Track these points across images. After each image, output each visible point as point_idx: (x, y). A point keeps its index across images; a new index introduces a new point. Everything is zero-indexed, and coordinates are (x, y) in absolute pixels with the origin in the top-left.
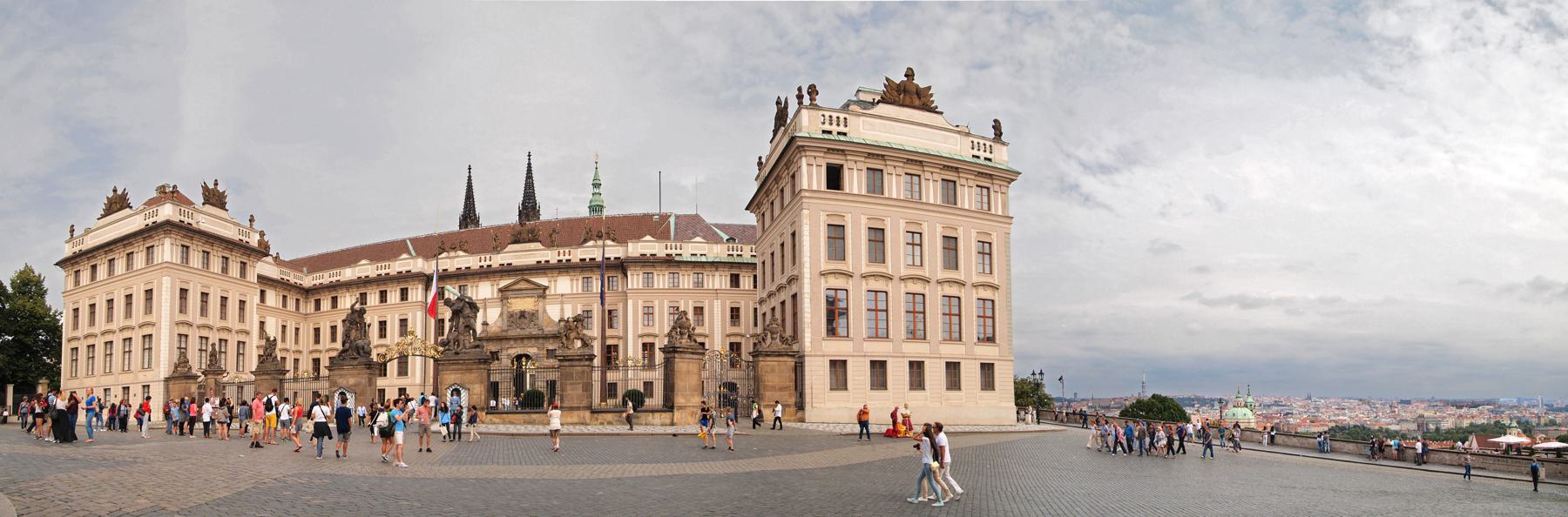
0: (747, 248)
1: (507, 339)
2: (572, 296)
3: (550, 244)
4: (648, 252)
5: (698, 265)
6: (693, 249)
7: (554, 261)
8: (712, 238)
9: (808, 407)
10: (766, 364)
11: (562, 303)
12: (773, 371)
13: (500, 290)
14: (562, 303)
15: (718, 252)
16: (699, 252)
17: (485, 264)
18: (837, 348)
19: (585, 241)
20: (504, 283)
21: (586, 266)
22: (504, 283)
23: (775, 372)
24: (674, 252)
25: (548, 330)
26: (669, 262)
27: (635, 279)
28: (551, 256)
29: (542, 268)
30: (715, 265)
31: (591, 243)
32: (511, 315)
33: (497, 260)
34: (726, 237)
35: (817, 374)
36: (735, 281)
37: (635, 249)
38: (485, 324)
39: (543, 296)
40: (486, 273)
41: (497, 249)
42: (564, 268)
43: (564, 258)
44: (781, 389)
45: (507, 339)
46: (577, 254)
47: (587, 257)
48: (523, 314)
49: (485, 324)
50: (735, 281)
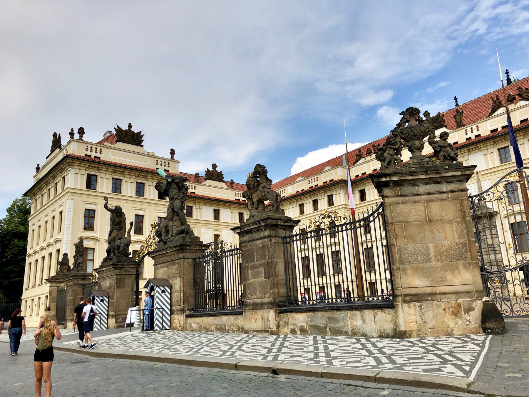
11: (478, 180)
19: (494, 110)
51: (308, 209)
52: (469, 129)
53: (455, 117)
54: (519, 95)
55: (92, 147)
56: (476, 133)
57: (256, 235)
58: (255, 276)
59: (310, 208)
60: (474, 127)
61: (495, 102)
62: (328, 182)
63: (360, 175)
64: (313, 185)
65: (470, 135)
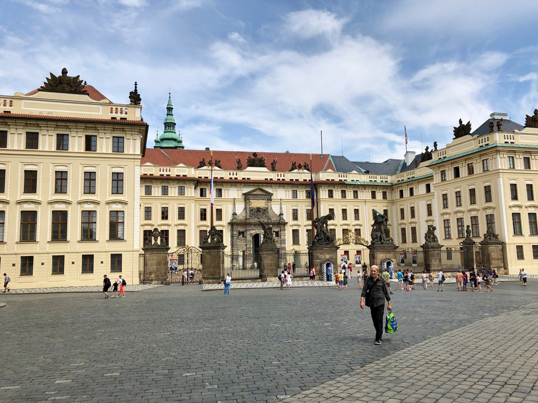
0: (378, 177)
1: (250, 224)
2: (287, 201)
3: (273, 169)
4: (331, 178)
5: (357, 187)
6: (352, 177)
7: (275, 179)
8: (360, 172)
9: (509, 267)
10: (492, 248)
11: (281, 204)
12: (494, 251)
13: (244, 194)
14: (281, 204)
15: (365, 179)
16: (355, 179)
17: (233, 177)
18: (519, 240)
19: (292, 169)
20: (246, 190)
21: (294, 184)
22: (246, 190)
23: (494, 251)
24: (343, 179)
25: (274, 219)
26: (342, 184)
27: (323, 194)
28: (274, 176)
29: (269, 183)
30: (364, 186)
31: (296, 171)
32: (251, 210)
33: (241, 175)
34: (363, 171)
35: (511, 253)
36: (374, 196)
37: (323, 176)
38: (234, 214)
39: (271, 200)
40: (234, 183)
41: (240, 168)
42: (281, 184)
43: (281, 178)
44: (498, 259)
45: (250, 224)
46: (288, 176)
47: (294, 179)
48: (259, 209)
49: (234, 214)
50: (374, 196)
51: (156, 192)
52: (279, 174)
53: (272, 164)
54: (305, 166)
55: (117, 109)
56: (282, 178)
57: (436, 249)
58: (435, 262)
59: (158, 191)
60: (282, 174)
61: (293, 165)
62: (181, 176)
63: (203, 178)
64: (165, 173)
65: (279, 177)
